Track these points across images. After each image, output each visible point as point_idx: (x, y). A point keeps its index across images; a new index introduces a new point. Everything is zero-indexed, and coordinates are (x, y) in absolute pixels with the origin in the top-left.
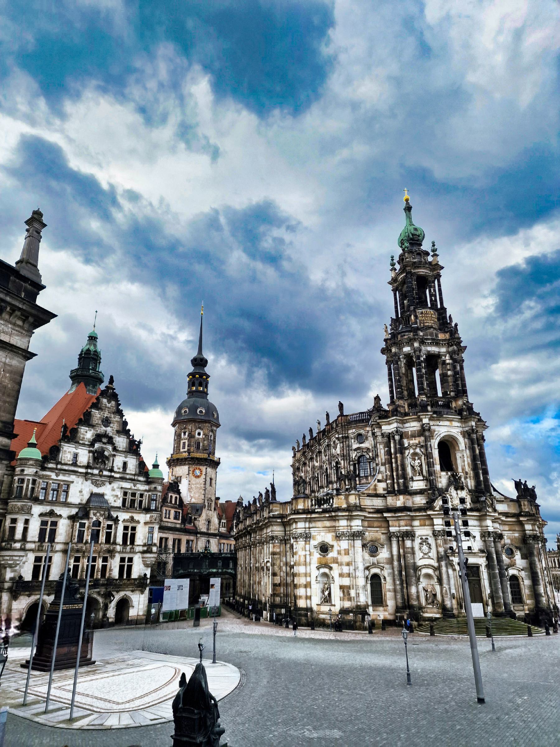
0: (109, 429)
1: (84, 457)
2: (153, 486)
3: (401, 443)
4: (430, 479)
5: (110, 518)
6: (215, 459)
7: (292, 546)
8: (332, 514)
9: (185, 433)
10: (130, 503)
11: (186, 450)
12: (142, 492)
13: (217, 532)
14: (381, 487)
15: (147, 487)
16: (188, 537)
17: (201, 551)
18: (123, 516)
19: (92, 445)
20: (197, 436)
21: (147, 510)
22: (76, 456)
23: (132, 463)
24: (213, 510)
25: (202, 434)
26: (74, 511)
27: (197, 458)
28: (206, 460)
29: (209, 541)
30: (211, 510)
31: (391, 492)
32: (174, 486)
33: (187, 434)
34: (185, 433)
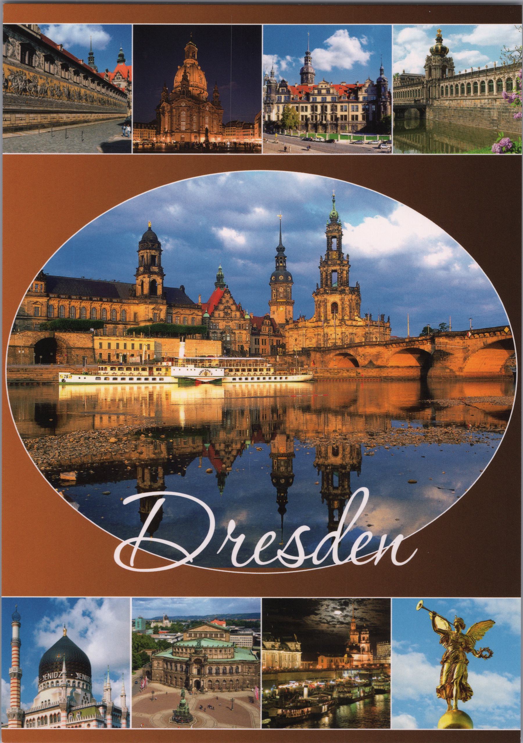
0: (228, 304)
1: (222, 314)
3: (319, 304)
4: (326, 316)
5: (233, 333)
8: (297, 328)
10: (240, 327)
14: (315, 319)
15: (244, 322)
18: (237, 332)
19: (224, 310)
21: (245, 329)
22: (219, 314)
23: (238, 314)
26: (221, 331)
31: (317, 321)
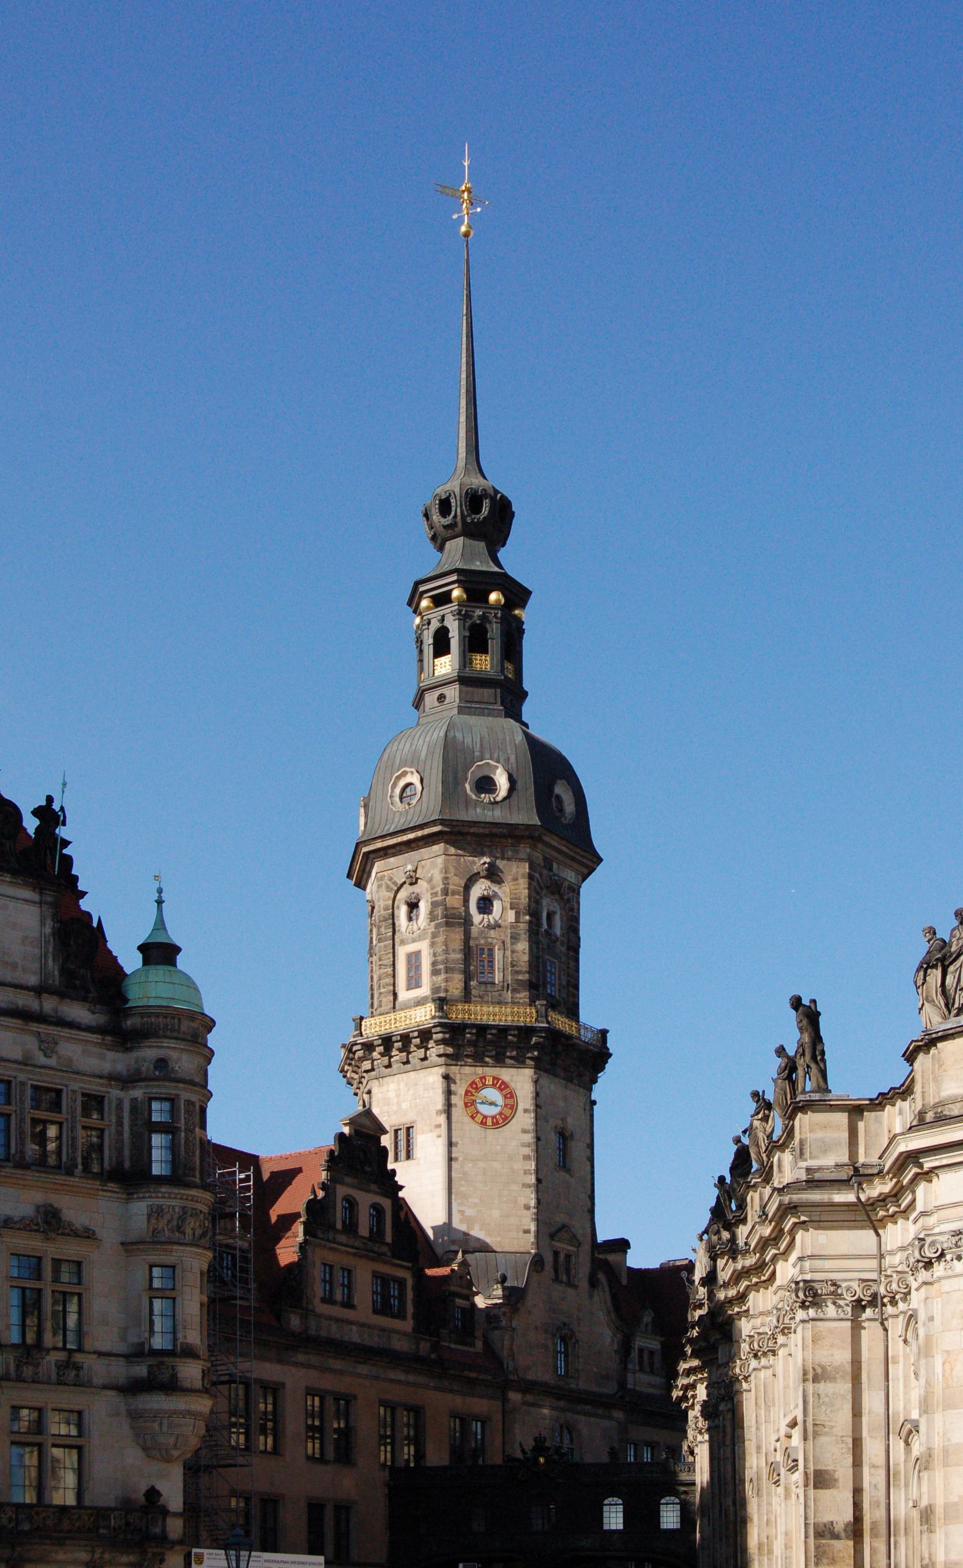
2: (148, 1053)
6: (586, 1036)
7: (912, 1317)
9: (413, 906)
11: (425, 990)
12: (94, 1087)
13: (610, 1388)
15: (116, 1061)
16: (458, 1400)
17: (519, 1455)
20: (477, 918)
24: (584, 1284)
25: (497, 905)
27: (482, 1029)
28: (526, 1032)
29: (570, 1428)
30: (570, 1284)
32: (363, 1153)
33: (424, 907)
34: (413, 906)
